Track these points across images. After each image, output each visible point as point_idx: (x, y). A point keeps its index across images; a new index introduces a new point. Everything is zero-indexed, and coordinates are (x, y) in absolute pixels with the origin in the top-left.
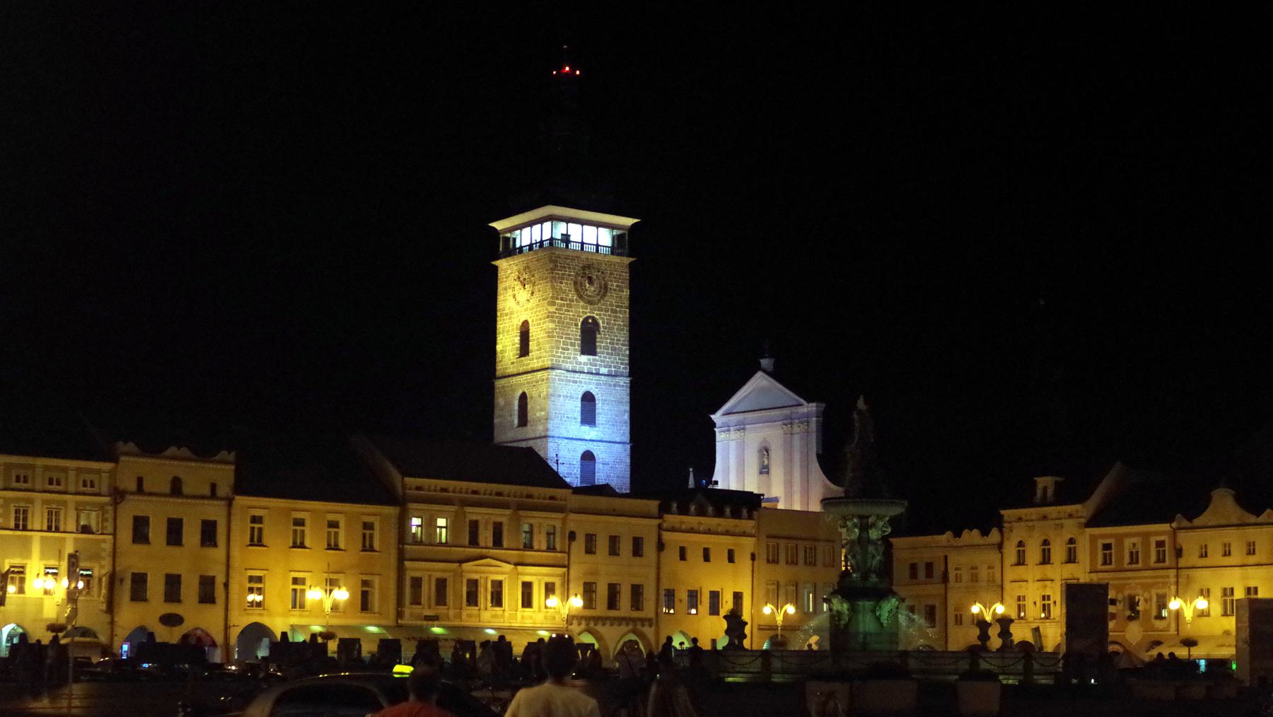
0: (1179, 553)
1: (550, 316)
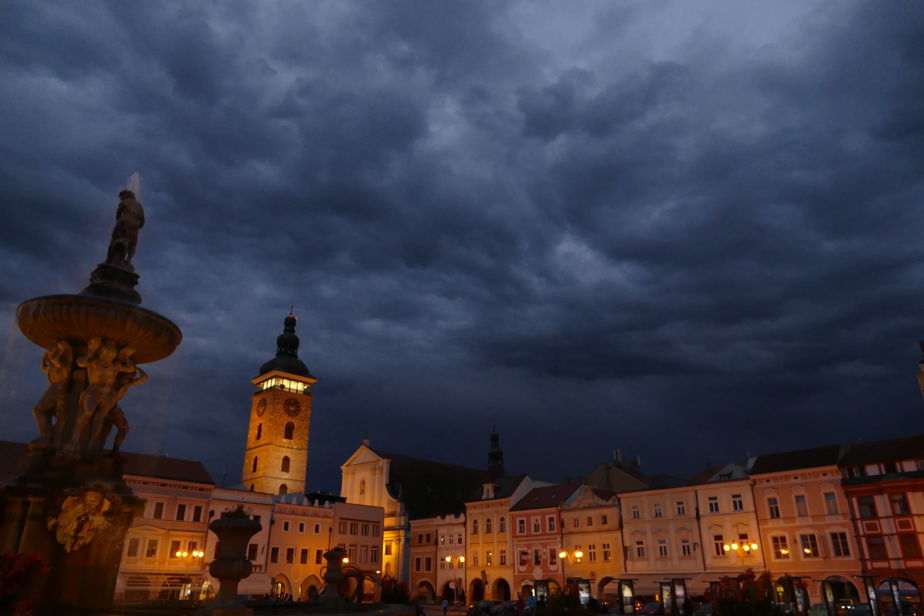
0: (562, 525)
1: (270, 420)
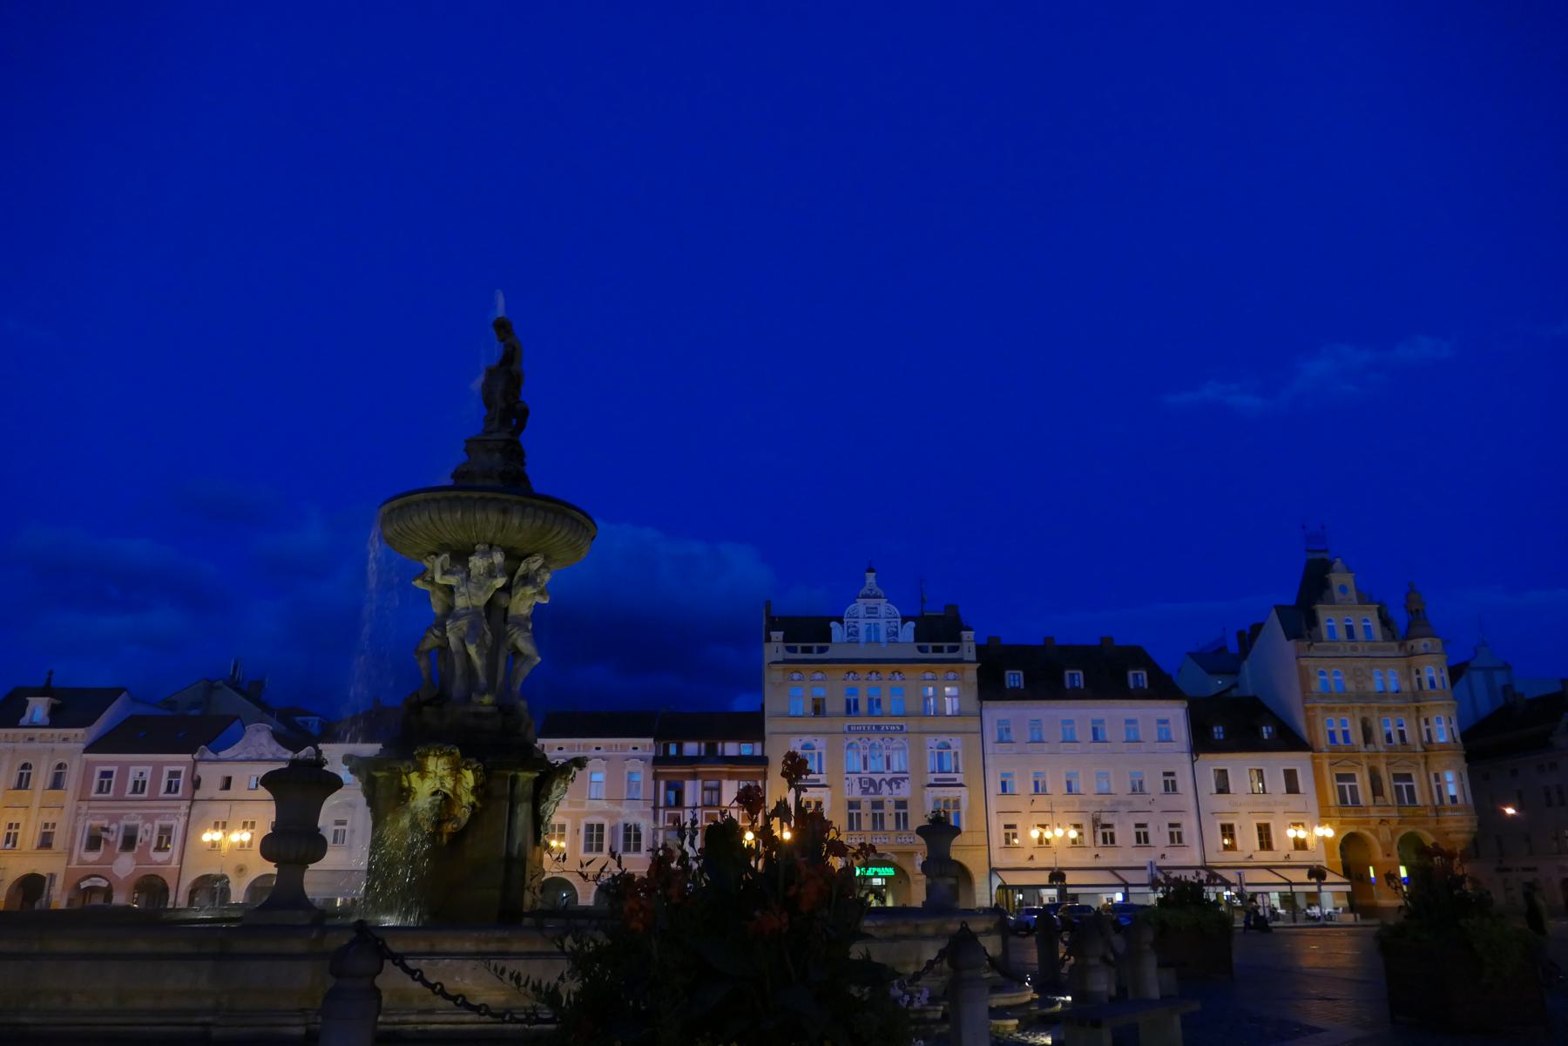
0: (196, 784)
